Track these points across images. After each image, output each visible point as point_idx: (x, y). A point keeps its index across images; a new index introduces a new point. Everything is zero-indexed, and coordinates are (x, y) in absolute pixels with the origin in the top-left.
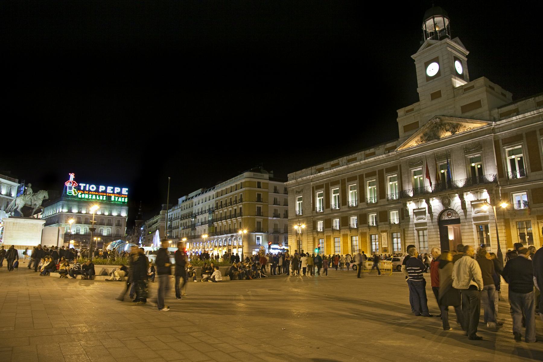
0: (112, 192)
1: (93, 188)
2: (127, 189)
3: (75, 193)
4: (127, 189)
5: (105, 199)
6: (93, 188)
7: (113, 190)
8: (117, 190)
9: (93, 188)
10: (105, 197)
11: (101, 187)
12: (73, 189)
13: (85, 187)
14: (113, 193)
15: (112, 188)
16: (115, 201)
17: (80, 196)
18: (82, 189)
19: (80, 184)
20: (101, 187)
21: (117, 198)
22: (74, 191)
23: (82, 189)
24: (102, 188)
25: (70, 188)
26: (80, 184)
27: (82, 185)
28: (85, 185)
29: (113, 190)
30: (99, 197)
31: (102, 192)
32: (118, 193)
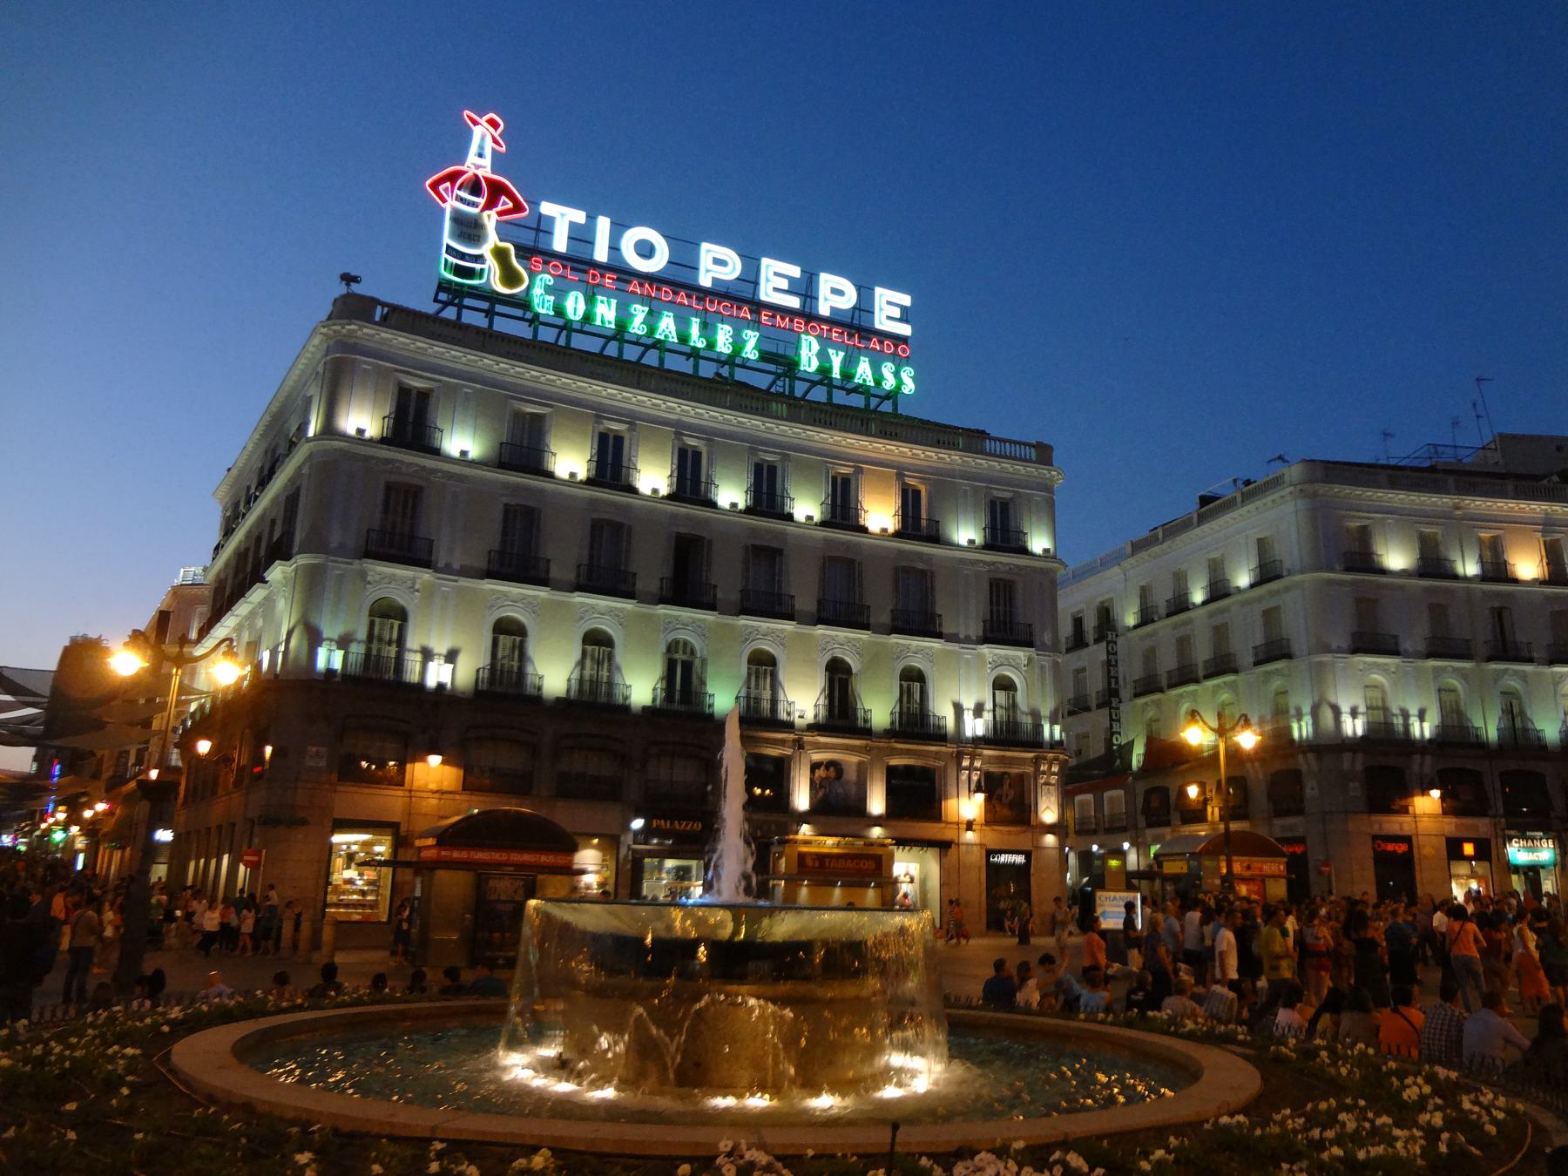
0: (794, 302)
1: (646, 250)
2: (906, 300)
3: (510, 277)
4: (906, 300)
5: (750, 352)
6: (646, 250)
7: (806, 289)
8: (835, 293)
9: (645, 247)
10: (751, 338)
11: (708, 252)
12: (492, 239)
13: (582, 236)
14: (809, 316)
15: (795, 271)
16: (825, 371)
17: (543, 304)
18: (560, 244)
19: (547, 208)
20: (708, 252)
21: (837, 359)
22: (500, 255)
23: (560, 244)
24: (717, 263)
25: (469, 229)
26: (547, 208)
27: (563, 218)
28: (580, 217)
29: (806, 289)
30: (707, 328)
31: (720, 293)
32: (834, 321)
